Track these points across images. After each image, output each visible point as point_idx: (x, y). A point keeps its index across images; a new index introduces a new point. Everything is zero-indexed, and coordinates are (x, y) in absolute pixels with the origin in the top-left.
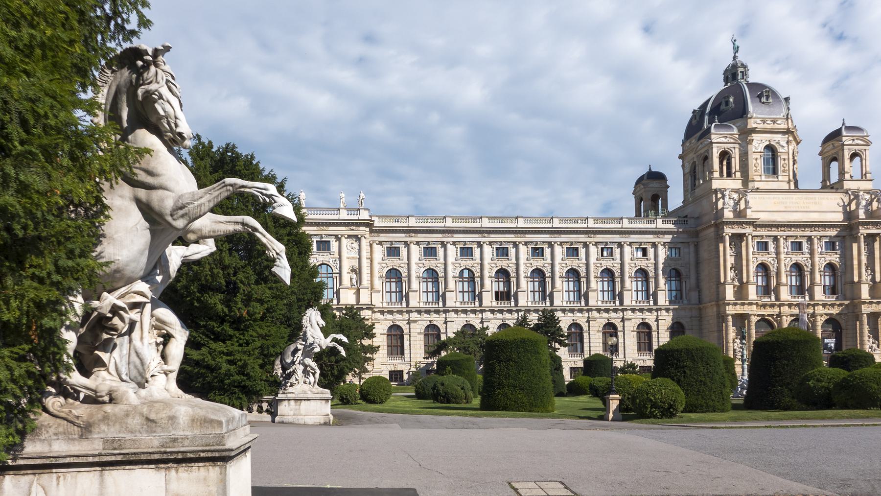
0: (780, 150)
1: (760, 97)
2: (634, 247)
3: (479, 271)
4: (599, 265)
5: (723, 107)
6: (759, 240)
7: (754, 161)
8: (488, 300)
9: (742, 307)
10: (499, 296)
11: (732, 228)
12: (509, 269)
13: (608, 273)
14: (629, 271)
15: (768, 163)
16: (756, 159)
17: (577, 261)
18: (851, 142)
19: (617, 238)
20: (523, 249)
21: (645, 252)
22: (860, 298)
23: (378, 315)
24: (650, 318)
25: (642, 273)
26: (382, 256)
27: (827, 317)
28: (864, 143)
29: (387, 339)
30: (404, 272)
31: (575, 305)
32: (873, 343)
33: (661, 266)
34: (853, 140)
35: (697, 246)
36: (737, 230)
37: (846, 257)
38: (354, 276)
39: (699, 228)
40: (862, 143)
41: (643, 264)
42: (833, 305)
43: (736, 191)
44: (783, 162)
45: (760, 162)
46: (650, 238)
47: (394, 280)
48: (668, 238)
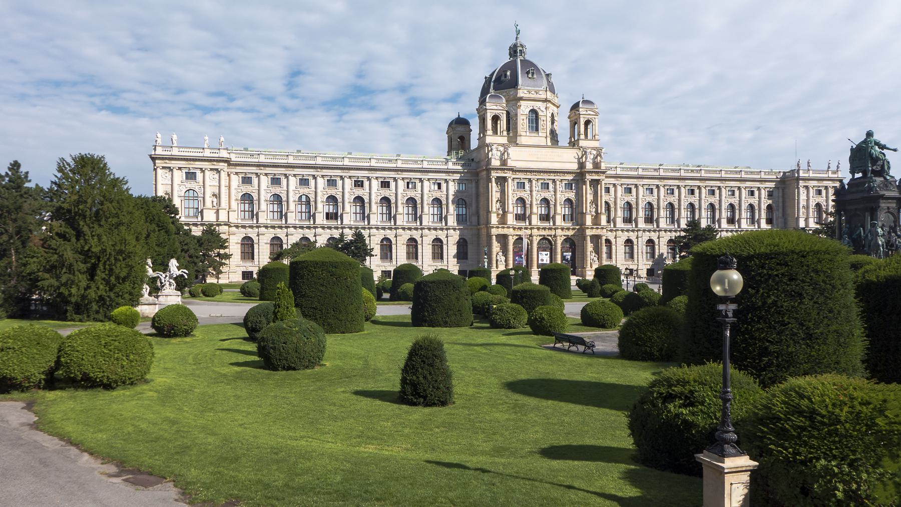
0: (540, 113)
1: (528, 73)
2: (431, 182)
3: (314, 197)
4: (405, 195)
5: (503, 78)
7: (522, 121)
8: (320, 219)
9: (503, 230)
10: (329, 216)
13: (411, 201)
14: (427, 200)
15: (532, 123)
17: (389, 191)
18: (585, 113)
19: (419, 175)
20: (347, 181)
21: (439, 187)
23: (234, 229)
24: (442, 235)
25: (437, 202)
29: (241, 247)
33: (451, 198)
35: (477, 182)
36: (501, 174)
38: (215, 200)
39: (478, 170)
41: (438, 194)
43: (503, 145)
44: (542, 122)
45: (526, 122)
46: (444, 176)
48: (457, 176)
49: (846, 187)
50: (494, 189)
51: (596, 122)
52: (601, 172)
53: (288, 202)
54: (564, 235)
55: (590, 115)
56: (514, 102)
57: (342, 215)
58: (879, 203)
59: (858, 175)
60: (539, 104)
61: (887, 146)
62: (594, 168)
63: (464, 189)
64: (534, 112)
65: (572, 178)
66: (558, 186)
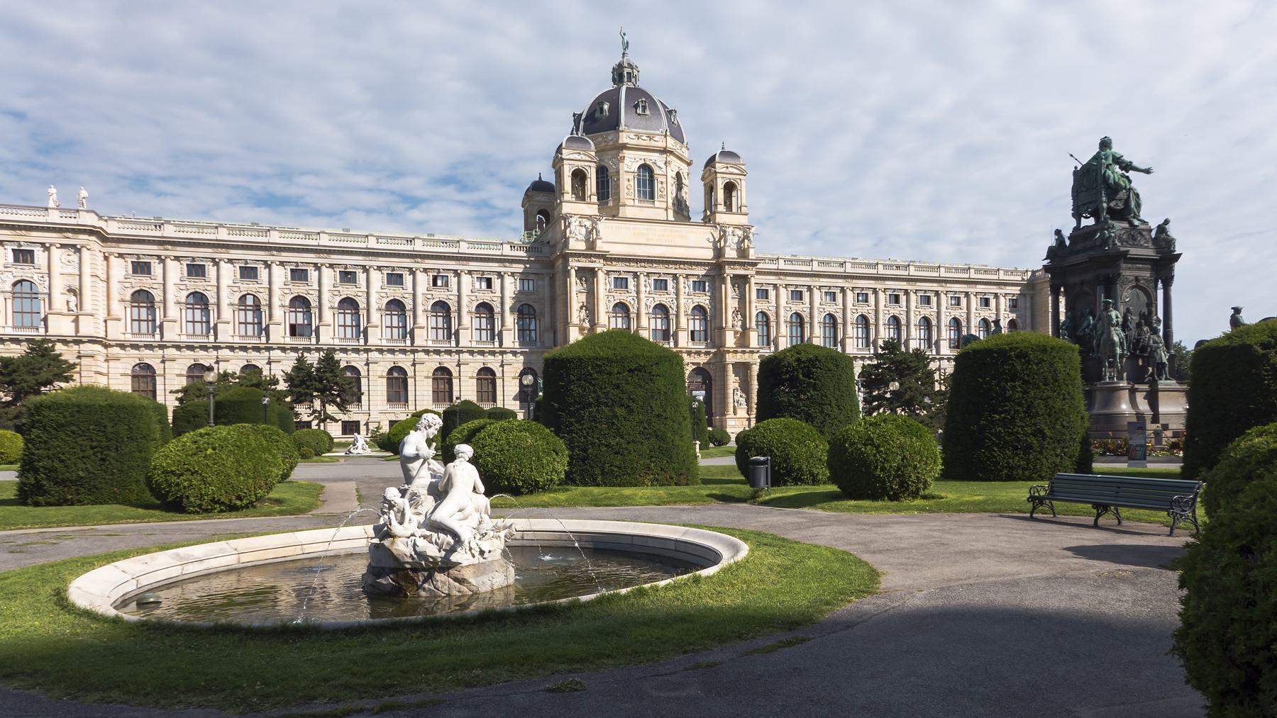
0: (657, 171)
1: (636, 107)
3: (267, 297)
4: (429, 296)
5: (597, 114)
6: (617, 276)
7: (627, 183)
8: (279, 334)
10: (294, 330)
11: (579, 261)
12: (449, 302)
13: (441, 307)
14: (468, 305)
15: (645, 186)
16: (629, 180)
17: (402, 291)
18: (724, 170)
19: (452, 265)
20: (327, 272)
21: (489, 285)
22: (724, 346)
23: (117, 350)
24: (493, 363)
25: (485, 309)
26: (180, 275)
27: (694, 367)
28: (739, 172)
30: (158, 296)
31: (348, 344)
32: (741, 396)
33: (509, 303)
34: (727, 167)
37: (716, 300)
38: (73, 299)
40: (736, 171)
41: (486, 297)
42: (698, 353)
43: (589, 217)
44: (660, 185)
45: (633, 184)
46: (495, 267)
47: (145, 305)
48: (519, 268)
49: (1068, 242)
50: (576, 288)
51: (743, 185)
52: (749, 264)
53: (218, 305)
54: (693, 364)
55: (732, 174)
56: (614, 152)
57: (317, 328)
58: (1119, 267)
59: (1089, 222)
60: (655, 156)
61: (1135, 164)
62: (739, 257)
63: (531, 289)
64: (645, 168)
65: (703, 272)
66: (681, 286)
